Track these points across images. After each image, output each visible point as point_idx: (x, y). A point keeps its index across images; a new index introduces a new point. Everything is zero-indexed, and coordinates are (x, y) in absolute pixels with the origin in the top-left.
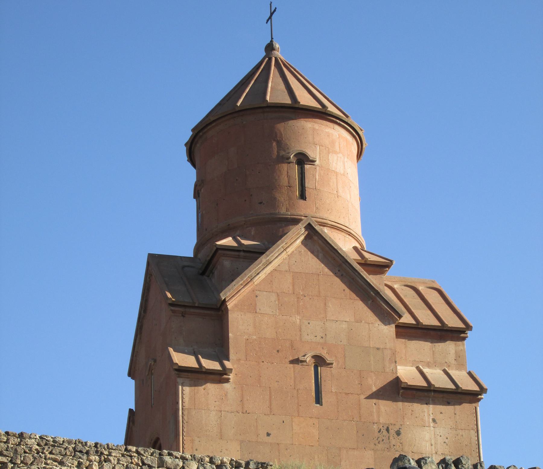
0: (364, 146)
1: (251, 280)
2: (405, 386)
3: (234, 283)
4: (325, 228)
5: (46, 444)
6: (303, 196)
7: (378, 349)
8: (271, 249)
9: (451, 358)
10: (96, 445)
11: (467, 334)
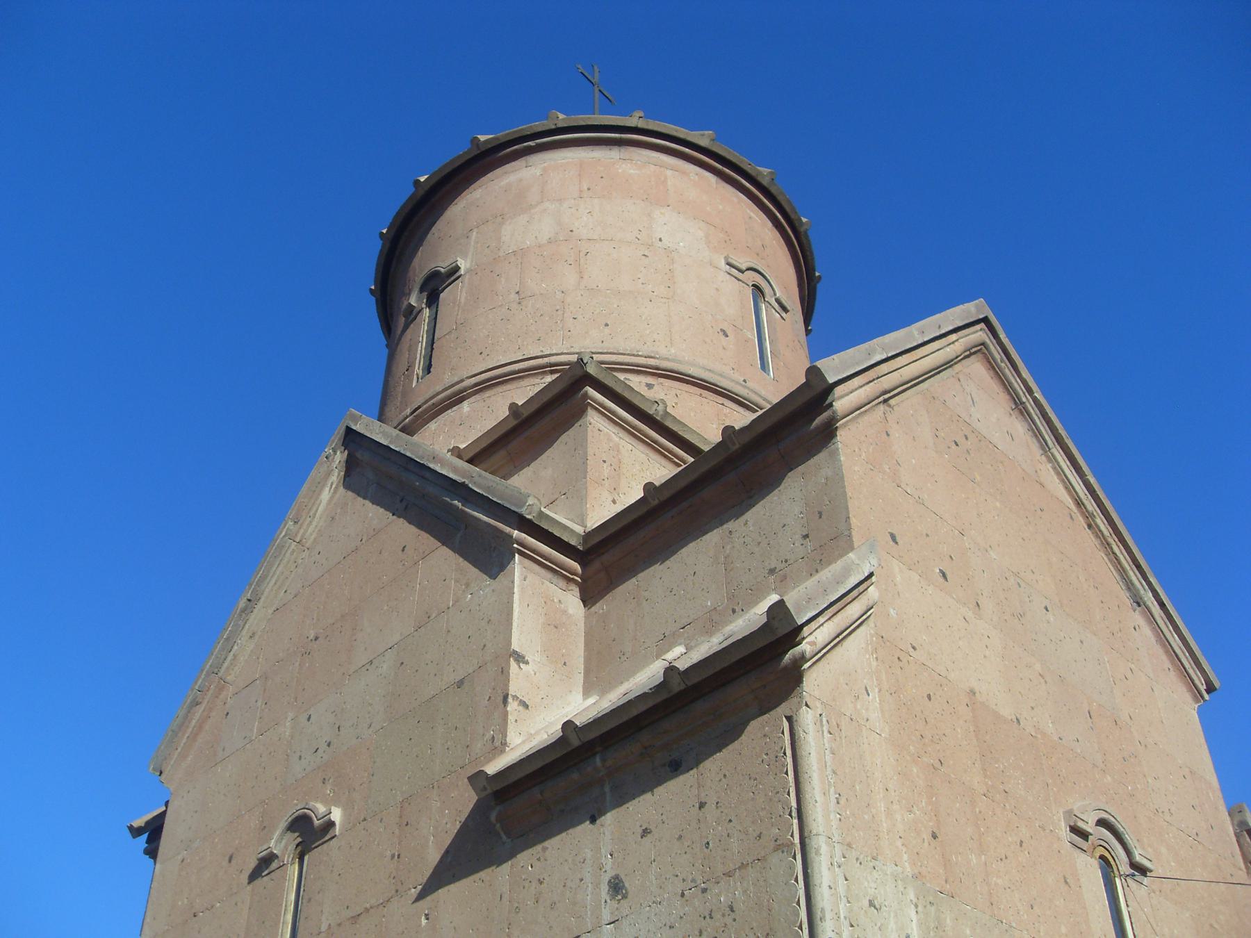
0: (704, 142)
2: (485, 789)
4: (465, 404)
6: (428, 369)
7: (460, 684)
11: (831, 405)
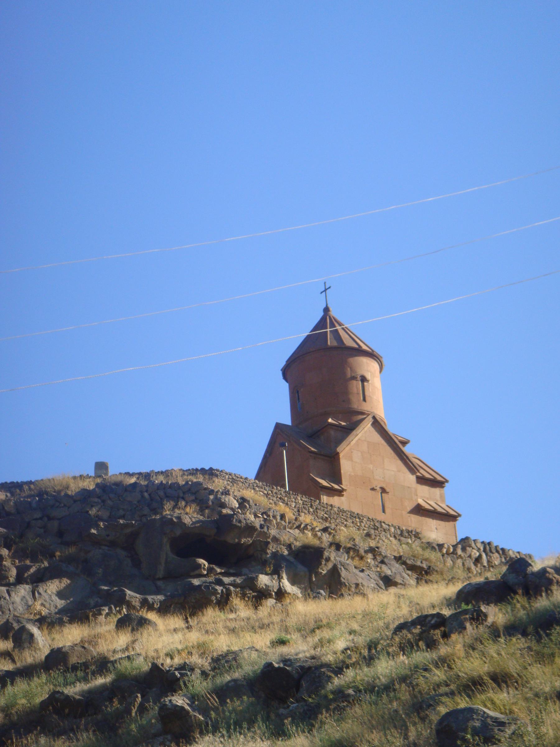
1: (350, 443)
3: (342, 444)
5: (341, 511)
6: (364, 400)
7: (409, 487)
8: (357, 428)
9: (438, 497)
10: (358, 514)
